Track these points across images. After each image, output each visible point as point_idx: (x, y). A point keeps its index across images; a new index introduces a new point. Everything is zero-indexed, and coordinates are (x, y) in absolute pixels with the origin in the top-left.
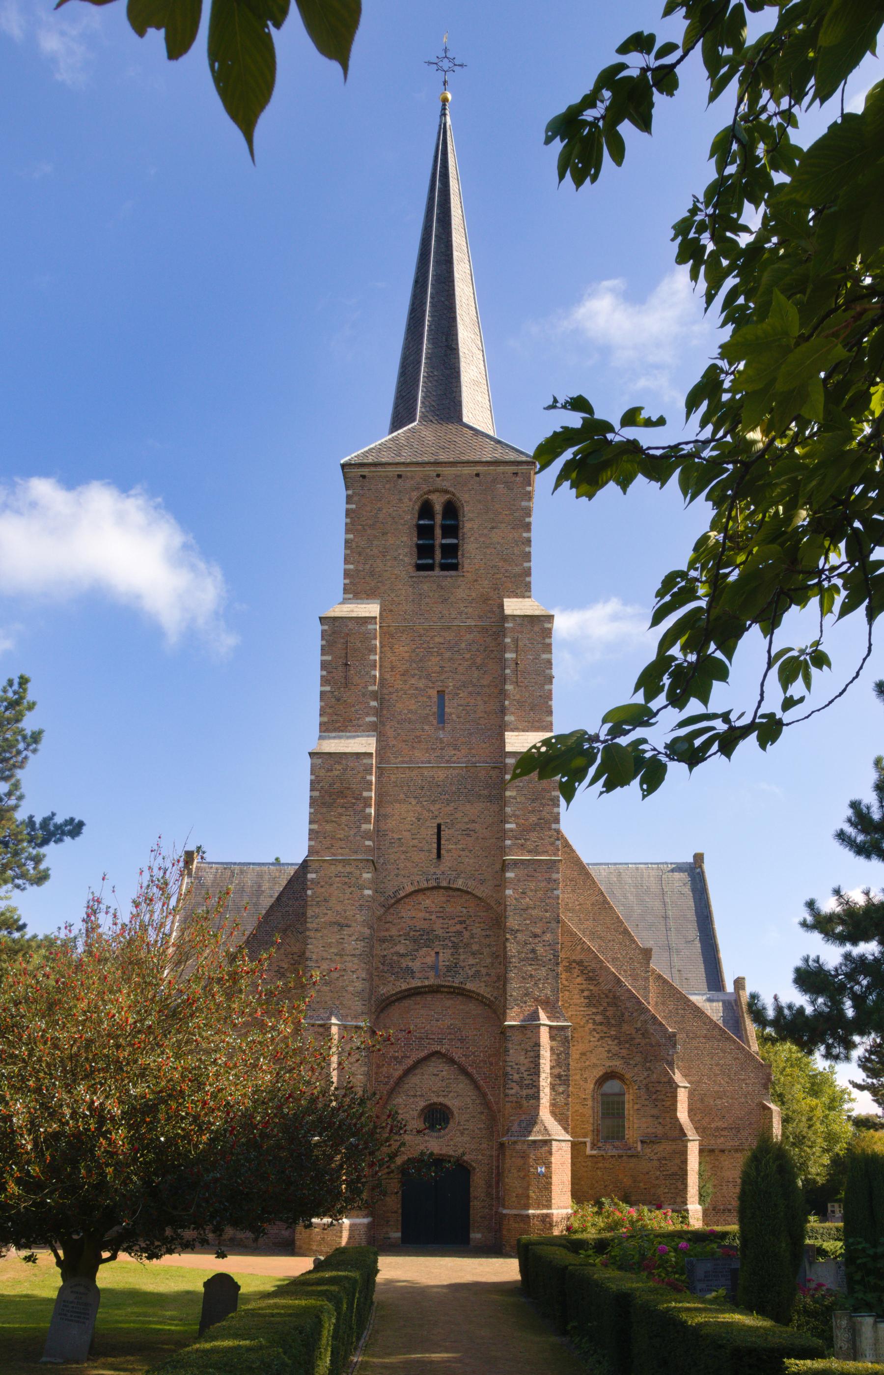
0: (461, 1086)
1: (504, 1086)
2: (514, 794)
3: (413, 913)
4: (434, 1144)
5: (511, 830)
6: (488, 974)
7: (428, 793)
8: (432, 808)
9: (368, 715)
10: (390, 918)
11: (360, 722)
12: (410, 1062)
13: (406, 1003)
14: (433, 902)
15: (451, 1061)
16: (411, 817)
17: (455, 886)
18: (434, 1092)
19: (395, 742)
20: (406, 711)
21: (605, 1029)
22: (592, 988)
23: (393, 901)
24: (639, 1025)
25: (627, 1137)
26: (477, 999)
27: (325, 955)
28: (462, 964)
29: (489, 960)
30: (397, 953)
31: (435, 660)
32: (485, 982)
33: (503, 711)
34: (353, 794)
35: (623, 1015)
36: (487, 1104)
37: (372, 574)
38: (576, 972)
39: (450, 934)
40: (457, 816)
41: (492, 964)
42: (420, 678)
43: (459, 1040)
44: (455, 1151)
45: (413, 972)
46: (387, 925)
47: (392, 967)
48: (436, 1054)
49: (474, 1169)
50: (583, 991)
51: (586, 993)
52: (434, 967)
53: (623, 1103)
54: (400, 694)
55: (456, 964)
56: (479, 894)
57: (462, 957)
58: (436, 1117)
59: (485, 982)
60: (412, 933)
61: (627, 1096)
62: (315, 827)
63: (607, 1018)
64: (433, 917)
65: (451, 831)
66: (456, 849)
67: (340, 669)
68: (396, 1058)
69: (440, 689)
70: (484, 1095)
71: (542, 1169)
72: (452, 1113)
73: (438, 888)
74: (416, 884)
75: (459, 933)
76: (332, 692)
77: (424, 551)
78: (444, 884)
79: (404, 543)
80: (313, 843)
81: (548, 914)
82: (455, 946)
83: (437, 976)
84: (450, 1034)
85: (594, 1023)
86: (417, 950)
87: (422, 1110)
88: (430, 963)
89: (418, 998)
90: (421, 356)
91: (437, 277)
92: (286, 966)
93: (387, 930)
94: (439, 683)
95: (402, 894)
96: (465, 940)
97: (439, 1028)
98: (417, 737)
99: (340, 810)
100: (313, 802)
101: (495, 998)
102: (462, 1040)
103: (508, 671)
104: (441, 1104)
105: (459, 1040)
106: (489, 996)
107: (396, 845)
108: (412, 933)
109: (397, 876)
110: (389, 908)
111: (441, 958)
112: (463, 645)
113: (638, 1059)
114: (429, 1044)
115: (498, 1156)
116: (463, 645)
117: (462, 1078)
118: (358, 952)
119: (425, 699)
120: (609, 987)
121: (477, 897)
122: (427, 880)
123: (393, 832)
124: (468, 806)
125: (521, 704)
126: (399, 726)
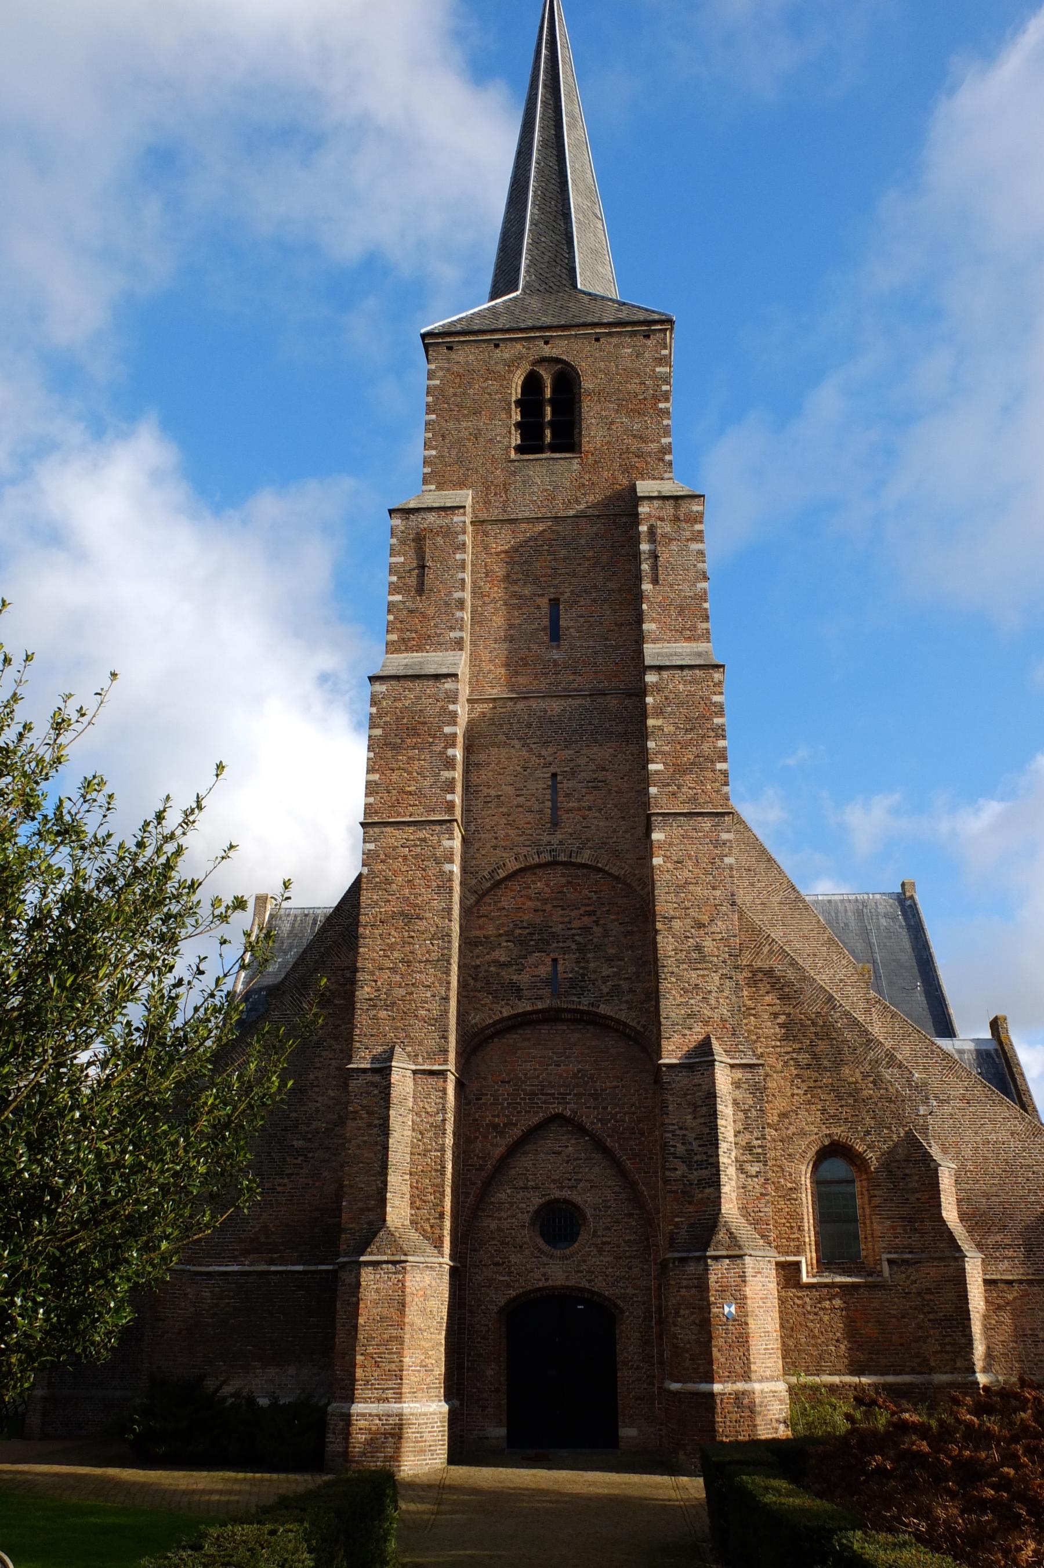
0: (596, 1170)
1: (663, 1167)
2: (659, 722)
4: (556, 1272)
5: (657, 772)
6: (631, 991)
7: (538, 733)
8: (544, 753)
10: (484, 910)
11: (442, 639)
12: (517, 1132)
13: (512, 1038)
14: (548, 885)
15: (580, 1130)
17: (579, 860)
18: (554, 1181)
25: (863, 1253)
26: (617, 1031)
28: (593, 977)
29: (632, 969)
30: (496, 962)
32: (627, 1002)
33: (639, 619)
38: (764, 987)
39: (573, 931)
40: (580, 761)
43: (590, 1095)
44: (590, 1281)
45: (519, 990)
46: (481, 921)
47: (488, 983)
49: (622, 1312)
50: (776, 1015)
51: (782, 1019)
52: (551, 981)
53: (853, 1196)
55: (583, 975)
56: (615, 871)
59: (627, 1002)
60: (518, 931)
61: (857, 1184)
62: (376, 777)
63: (815, 1056)
65: (571, 784)
66: (579, 809)
68: (495, 1126)
69: (552, 596)
71: (730, 1309)
72: (584, 1217)
73: (554, 864)
75: (586, 930)
76: (403, 602)
78: (563, 858)
81: (718, 893)
82: (582, 949)
83: (556, 994)
84: (577, 1085)
85: (798, 1065)
86: (525, 957)
87: (536, 1212)
88: (544, 975)
90: (524, 223)
91: (544, 143)
93: (481, 928)
94: (552, 590)
95: (502, 874)
96: (595, 940)
97: (560, 1076)
101: (644, 1026)
104: (566, 1201)
105: (590, 1095)
106: (634, 1024)
107: (492, 805)
108: (518, 931)
109: (495, 848)
110: (484, 895)
111: (560, 968)
114: (544, 1102)
115: (659, 1289)
116: (583, 542)
119: (532, 610)
121: (611, 875)
122: (539, 854)
123: (489, 787)
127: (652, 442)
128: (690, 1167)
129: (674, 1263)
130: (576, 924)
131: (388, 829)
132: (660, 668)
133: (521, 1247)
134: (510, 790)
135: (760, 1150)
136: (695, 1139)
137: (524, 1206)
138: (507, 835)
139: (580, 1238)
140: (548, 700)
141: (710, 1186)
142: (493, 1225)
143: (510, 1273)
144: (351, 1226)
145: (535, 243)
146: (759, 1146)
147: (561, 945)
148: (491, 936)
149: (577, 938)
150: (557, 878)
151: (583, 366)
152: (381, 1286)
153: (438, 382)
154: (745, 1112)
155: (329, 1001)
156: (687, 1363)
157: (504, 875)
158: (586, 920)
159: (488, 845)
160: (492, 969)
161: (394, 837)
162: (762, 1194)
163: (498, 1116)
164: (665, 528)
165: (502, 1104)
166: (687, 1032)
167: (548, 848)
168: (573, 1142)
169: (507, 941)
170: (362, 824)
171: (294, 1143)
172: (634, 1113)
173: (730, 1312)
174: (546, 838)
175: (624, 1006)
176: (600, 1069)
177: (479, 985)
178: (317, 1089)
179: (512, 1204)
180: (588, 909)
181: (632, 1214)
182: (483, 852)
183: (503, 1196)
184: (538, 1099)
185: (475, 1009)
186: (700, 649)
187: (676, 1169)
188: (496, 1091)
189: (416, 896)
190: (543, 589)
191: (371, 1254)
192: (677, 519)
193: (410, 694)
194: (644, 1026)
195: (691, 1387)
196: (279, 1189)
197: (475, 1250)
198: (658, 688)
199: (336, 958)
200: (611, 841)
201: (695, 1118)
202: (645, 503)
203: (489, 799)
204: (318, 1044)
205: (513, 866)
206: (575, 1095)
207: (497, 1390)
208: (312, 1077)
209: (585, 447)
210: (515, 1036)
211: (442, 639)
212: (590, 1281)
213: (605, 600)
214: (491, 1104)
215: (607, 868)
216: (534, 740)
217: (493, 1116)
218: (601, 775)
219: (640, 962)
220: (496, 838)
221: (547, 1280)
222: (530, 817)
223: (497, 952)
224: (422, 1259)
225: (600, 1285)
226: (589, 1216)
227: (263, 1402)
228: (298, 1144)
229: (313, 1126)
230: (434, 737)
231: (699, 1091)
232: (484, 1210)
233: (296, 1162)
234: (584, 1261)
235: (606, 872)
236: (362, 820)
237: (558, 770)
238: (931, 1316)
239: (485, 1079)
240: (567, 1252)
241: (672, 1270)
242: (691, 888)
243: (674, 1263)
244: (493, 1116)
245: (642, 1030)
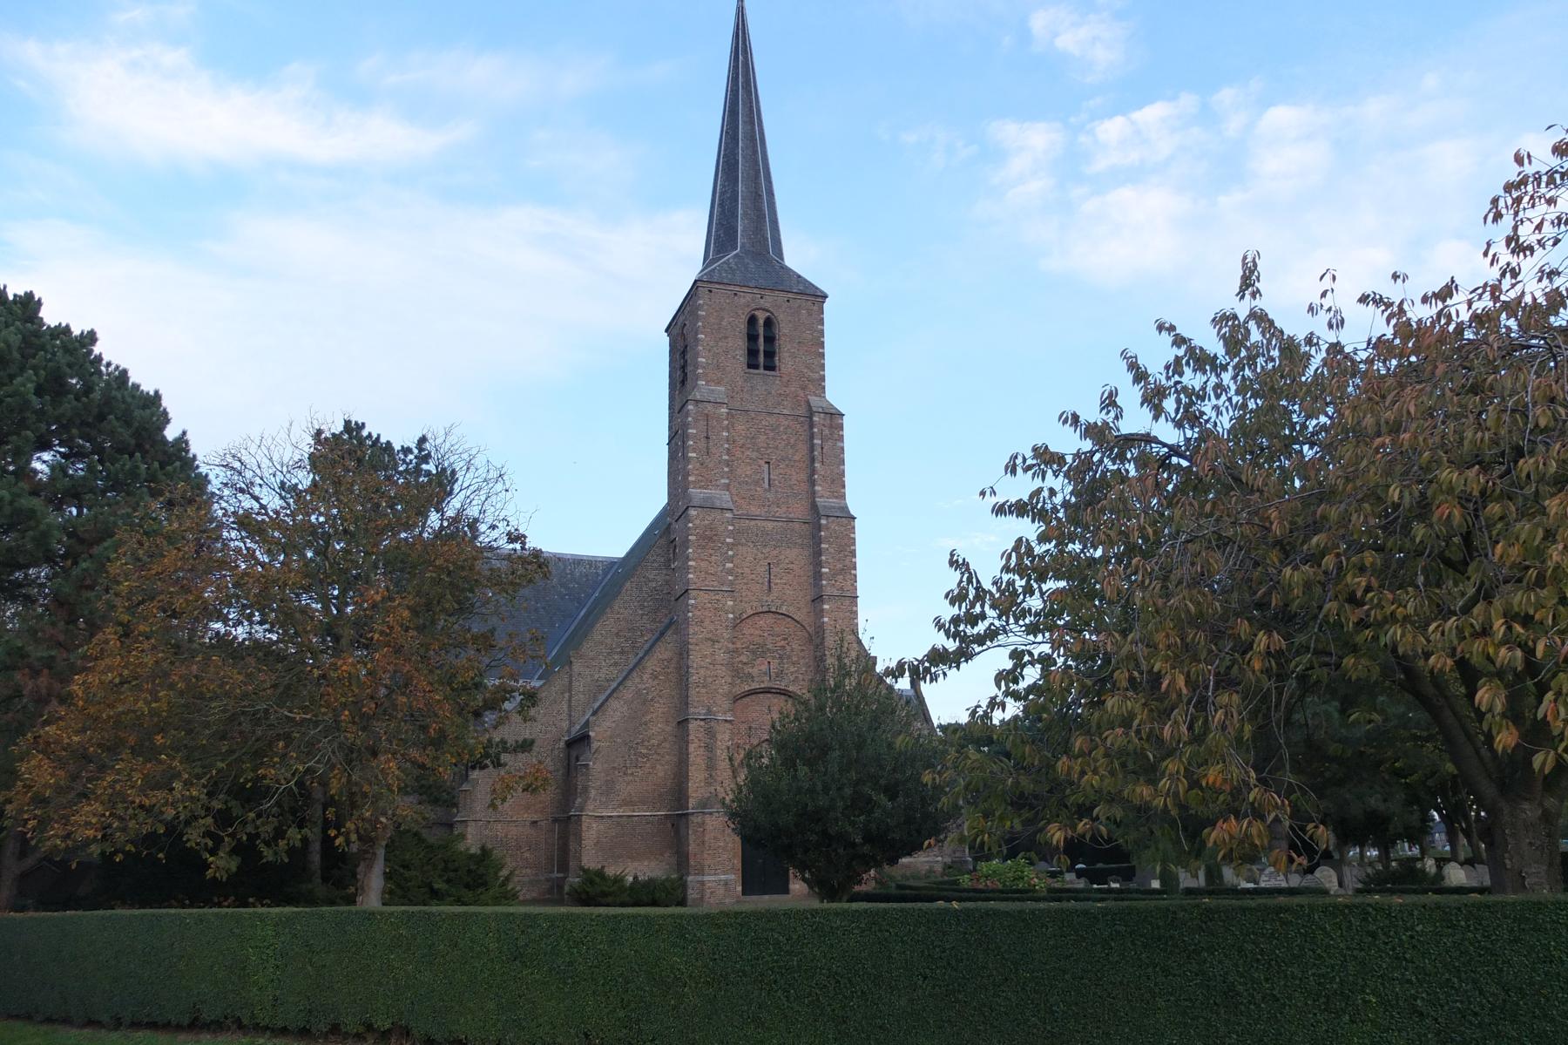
13: (746, 700)
77: (752, 353)
134: (747, 570)
145: (745, 214)
150: (770, 619)
151: (781, 317)
164: (826, 432)
205: (750, 612)
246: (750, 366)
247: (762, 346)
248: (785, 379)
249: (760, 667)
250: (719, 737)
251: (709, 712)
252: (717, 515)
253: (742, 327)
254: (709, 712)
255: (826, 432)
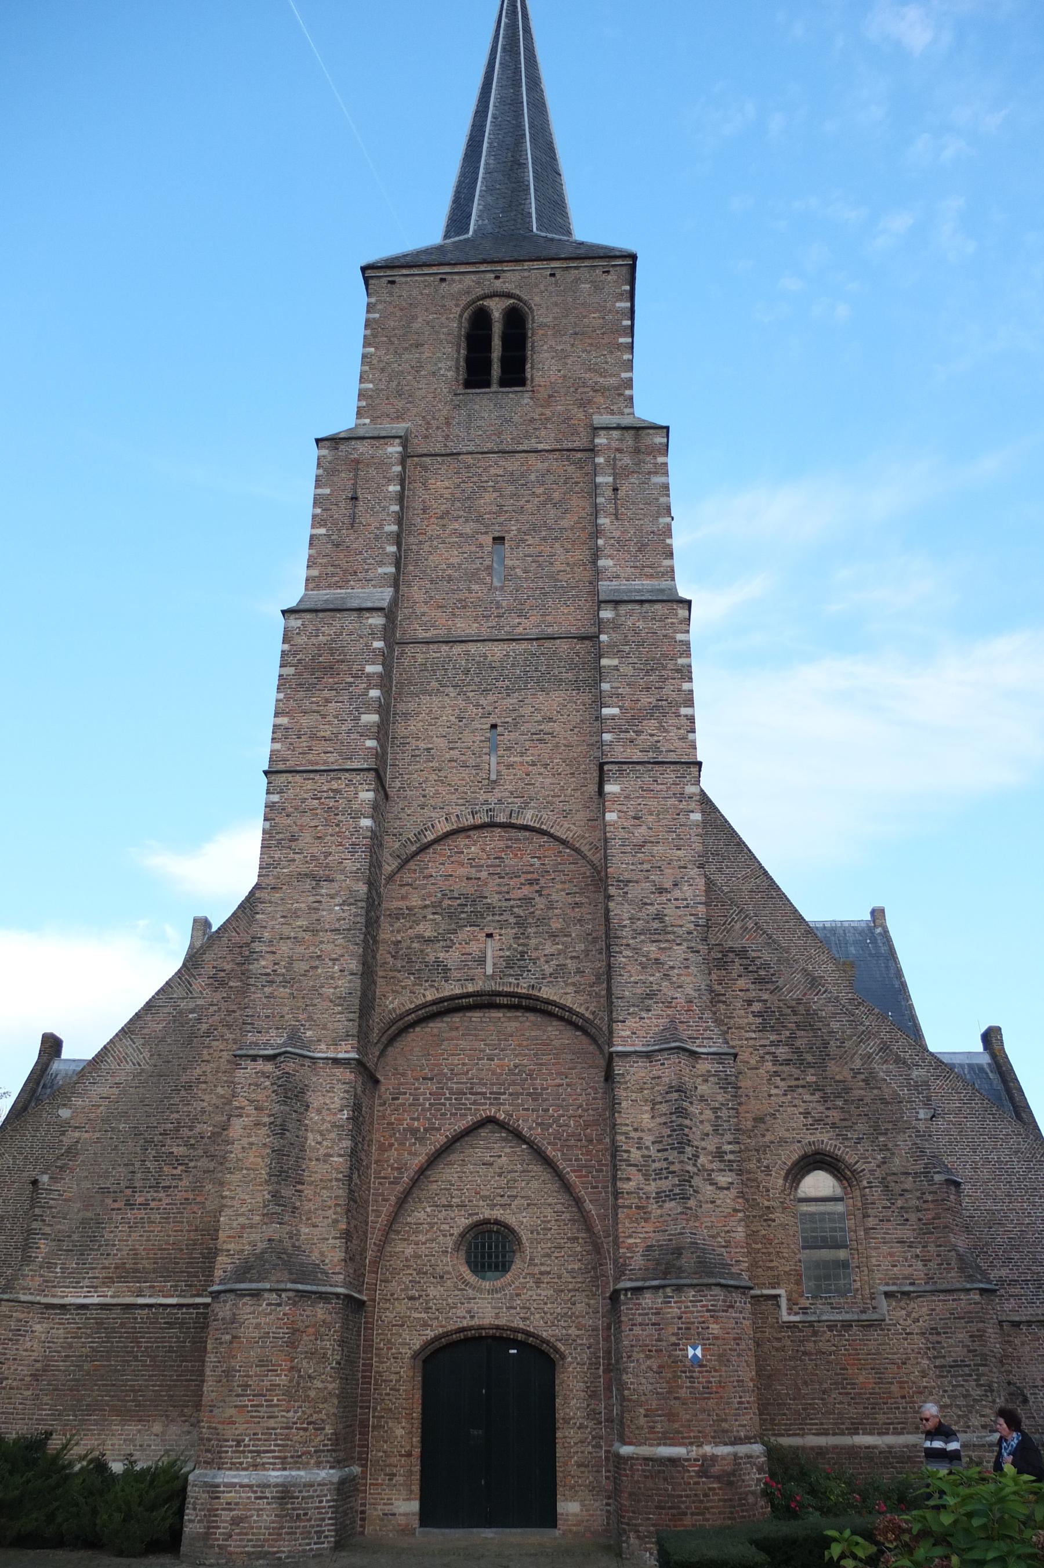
0: (535, 1184)
3: (449, 868)
5: (613, 718)
6: (579, 971)
9: (381, 564)
11: (371, 574)
12: (440, 1139)
13: (436, 1026)
14: (483, 850)
15: (518, 1136)
16: (448, 716)
17: (520, 822)
18: (484, 1198)
19: (425, 609)
20: (445, 566)
21: (796, 1072)
22: (765, 997)
23: (414, 848)
24: (858, 1064)
26: (561, 1019)
27: (286, 931)
28: (534, 955)
30: (419, 937)
31: (489, 497)
32: (574, 984)
34: (350, 669)
35: (826, 1044)
36: (584, 1219)
37: (400, 394)
38: (737, 968)
39: (512, 903)
40: (522, 711)
41: (587, 952)
42: (467, 521)
43: (529, 1094)
44: (524, 1319)
45: (446, 969)
46: (404, 890)
48: (491, 1120)
49: (563, 1357)
51: (757, 1007)
54: (435, 543)
55: (522, 954)
56: (560, 833)
57: (533, 942)
58: (489, 1248)
59: (574, 984)
62: (284, 720)
63: (798, 1051)
64: (484, 875)
65: (513, 736)
66: (522, 764)
67: (342, 505)
68: (414, 1131)
69: (497, 534)
70: (578, 1202)
74: (454, 819)
75: (527, 901)
76: (329, 536)
78: (502, 818)
79: (445, 360)
80: (278, 746)
85: (775, 1062)
87: (463, 1235)
89: (456, 1018)
91: (502, 100)
92: (228, 967)
94: (497, 528)
95: (430, 836)
96: (538, 912)
97: (494, 1073)
98: (460, 600)
99: (326, 693)
100: (283, 682)
101: (593, 1013)
102: (535, 1096)
103: (600, 500)
104: (497, 1222)
105: (529, 1094)
106: (582, 1010)
110: (407, 861)
112: (533, 477)
113: (862, 1127)
114: (474, 1103)
116: (533, 477)
117: (537, 1168)
118: (344, 925)
119: (473, 548)
120: (798, 994)
124: (541, 697)
125: (621, 544)
126: (433, 587)
127: (611, 376)
128: (646, 1176)
129: (626, 1295)
130: (519, 894)
131: (298, 778)
132: (617, 603)
133: (442, 1277)
135: (731, 1157)
136: (653, 1143)
137: (447, 1227)
138: (437, 793)
139: (513, 1267)
140: (490, 644)
141: (671, 1200)
142: (409, 1251)
143: (427, 1310)
144: (229, 1247)
146: (732, 1152)
147: (497, 918)
148: (415, 907)
149: (516, 910)
150: (494, 840)
152: (263, 1320)
153: (377, 316)
154: (715, 1110)
155: (223, 984)
156: (642, 1421)
157: (432, 837)
158: (526, 891)
159: (415, 804)
160: (415, 945)
161: (301, 787)
162: (736, 1210)
163: (418, 1119)
165: (423, 1105)
166: (644, 1014)
167: (485, 807)
168: (508, 1150)
169: (434, 913)
170: (266, 773)
171: (175, 1150)
172: (580, 1116)
173: (695, 1355)
174: (482, 797)
175: (570, 989)
176: (541, 1064)
177: (399, 964)
178: (204, 1086)
179: (432, 1225)
180: (529, 876)
181: (577, 1238)
182: (409, 812)
183: (422, 1215)
184: (466, 1099)
185: (393, 991)
186: (662, 587)
187: (629, 1179)
188: (416, 1089)
189: (328, 854)
190: (487, 526)
191: (251, 1281)
192: (637, 451)
193: (328, 629)
194: (593, 1013)
195: (645, 1451)
196: (153, 1204)
197: (386, 1281)
198: (615, 625)
199: (234, 934)
200: (557, 800)
201: (653, 1117)
202: (602, 433)
203: (417, 752)
204: (208, 1034)
205: (443, 827)
206: (511, 1094)
207: (409, 1455)
208: (198, 1071)
209: (538, 380)
210: (440, 1025)
211: (371, 574)
212: (524, 1319)
213: (556, 539)
214: (410, 1105)
215: (552, 831)
216: (471, 688)
217: (412, 1119)
218: (546, 727)
219: (590, 937)
220: (424, 796)
221: (472, 1317)
222: (465, 773)
223: (421, 926)
224: (314, 1288)
225: (538, 1325)
226: (524, 1240)
227: (117, 1467)
228: (179, 1150)
229: (197, 1130)
230: (356, 677)
231: (657, 1084)
232: (398, 1232)
233: (175, 1172)
234: (518, 1295)
235: (551, 836)
236: (266, 768)
237: (498, 721)
238: (938, 1362)
239: (403, 1075)
240: (498, 1284)
241: (625, 1304)
242: (648, 846)
243: (626, 1295)
244: (412, 1119)
245: (591, 1017)
246: (468, 384)
247: (495, 353)
248: (543, 394)
249: (471, 941)
250: (316, 1100)
251: (294, 1037)
252: (349, 621)
253: (453, 323)
254: (294, 1037)
255: (626, 460)
